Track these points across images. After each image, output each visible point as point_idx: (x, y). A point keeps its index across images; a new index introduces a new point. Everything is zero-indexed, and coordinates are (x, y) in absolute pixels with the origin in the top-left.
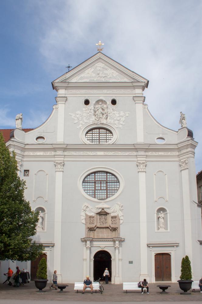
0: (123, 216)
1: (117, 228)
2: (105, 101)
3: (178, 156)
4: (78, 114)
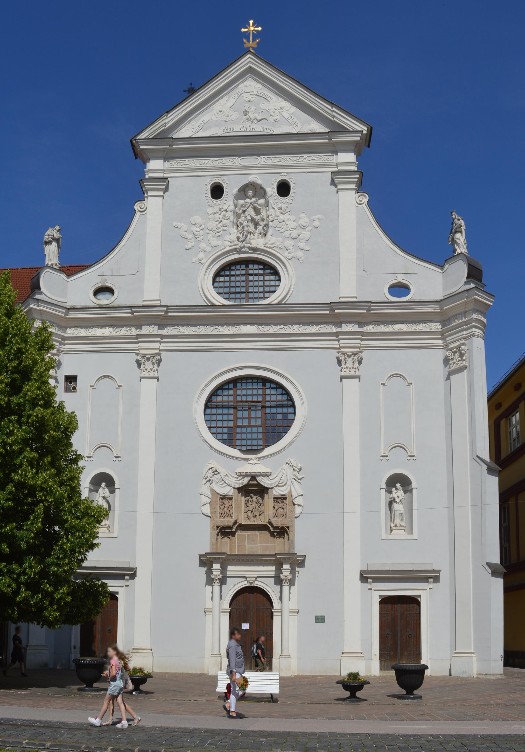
0: (302, 495)
1: (288, 527)
2: (262, 188)
3: (442, 333)
4: (195, 225)
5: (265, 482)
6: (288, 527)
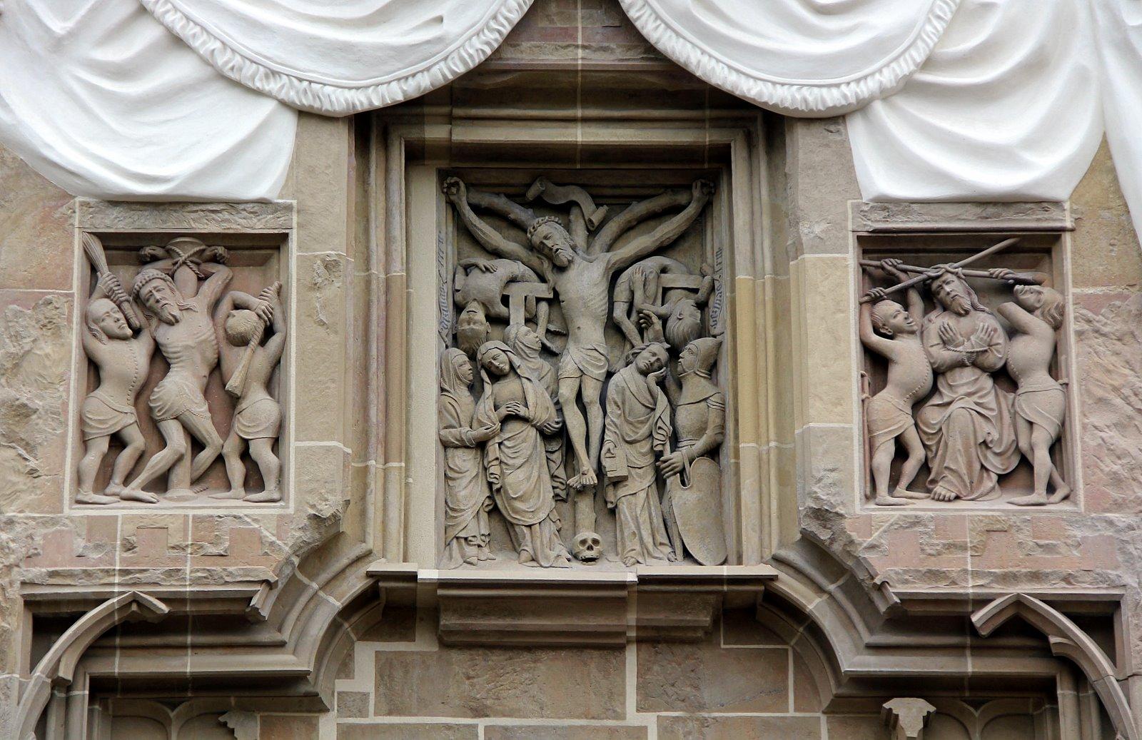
1: (1100, 618)
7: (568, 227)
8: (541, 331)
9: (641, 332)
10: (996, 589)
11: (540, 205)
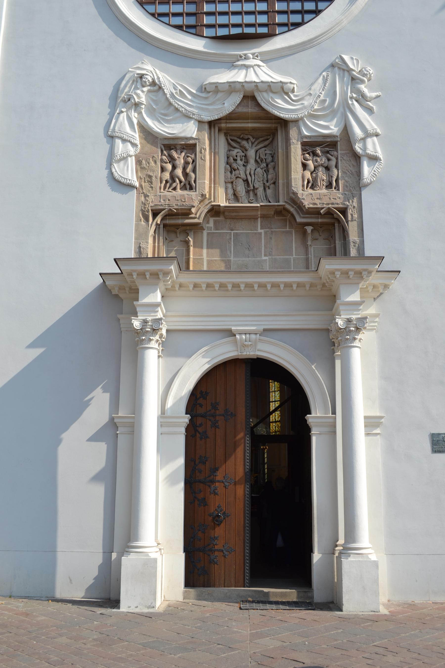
5: (281, 107)
6: (344, 211)
7: (248, 143)
8: (243, 161)
9: (261, 161)
10: (325, 206)
11: (243, 139)
